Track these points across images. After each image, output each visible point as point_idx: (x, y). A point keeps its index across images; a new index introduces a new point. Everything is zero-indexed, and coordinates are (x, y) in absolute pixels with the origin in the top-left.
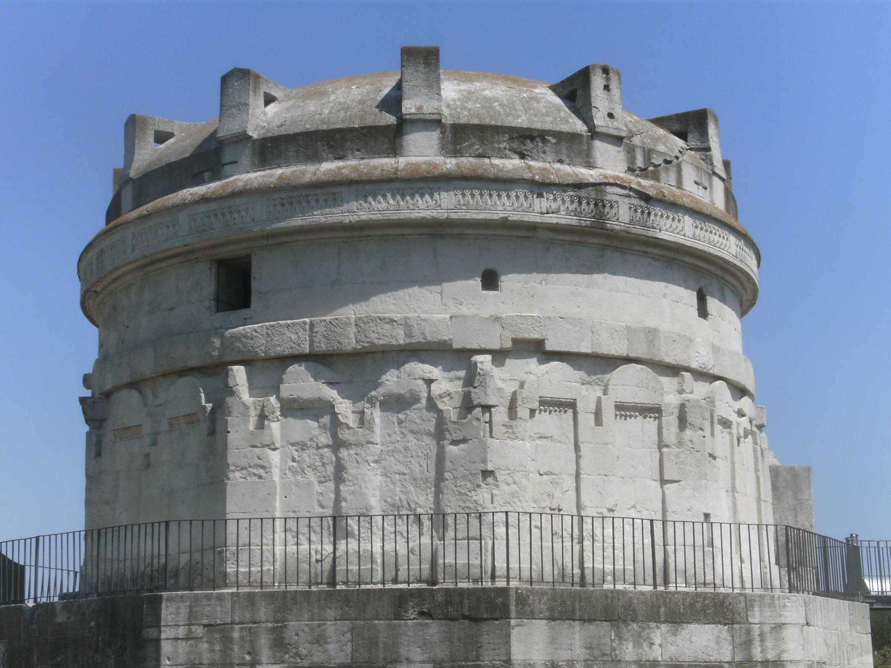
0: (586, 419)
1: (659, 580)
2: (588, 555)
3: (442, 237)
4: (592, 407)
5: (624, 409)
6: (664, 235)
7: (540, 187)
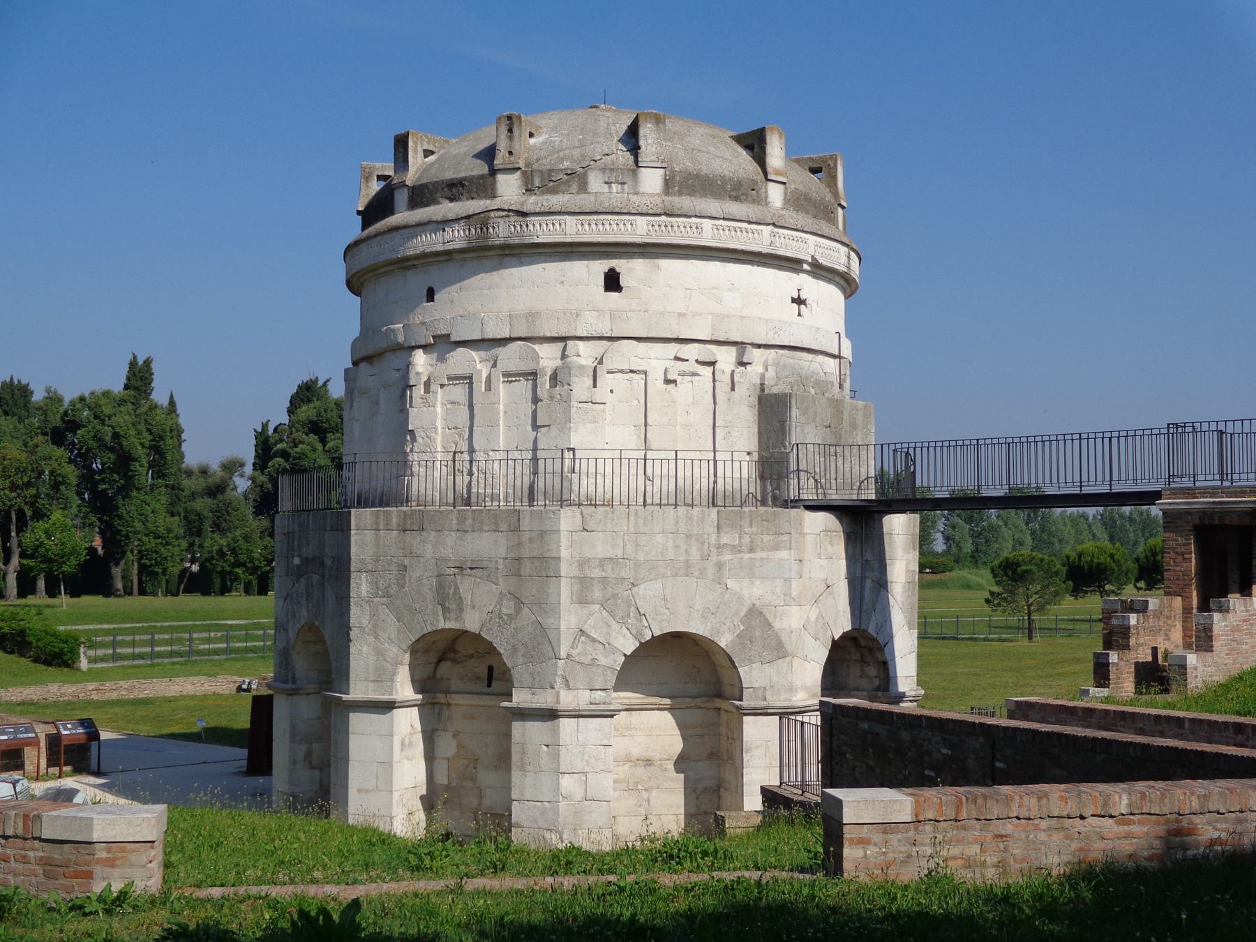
0: (480, 387)
1: (511, 499)
2: (474, 483)
3: (407, 268)
4: (484, 375)
5: (510, 376)
6: (542, 239)
7: (444, 223)
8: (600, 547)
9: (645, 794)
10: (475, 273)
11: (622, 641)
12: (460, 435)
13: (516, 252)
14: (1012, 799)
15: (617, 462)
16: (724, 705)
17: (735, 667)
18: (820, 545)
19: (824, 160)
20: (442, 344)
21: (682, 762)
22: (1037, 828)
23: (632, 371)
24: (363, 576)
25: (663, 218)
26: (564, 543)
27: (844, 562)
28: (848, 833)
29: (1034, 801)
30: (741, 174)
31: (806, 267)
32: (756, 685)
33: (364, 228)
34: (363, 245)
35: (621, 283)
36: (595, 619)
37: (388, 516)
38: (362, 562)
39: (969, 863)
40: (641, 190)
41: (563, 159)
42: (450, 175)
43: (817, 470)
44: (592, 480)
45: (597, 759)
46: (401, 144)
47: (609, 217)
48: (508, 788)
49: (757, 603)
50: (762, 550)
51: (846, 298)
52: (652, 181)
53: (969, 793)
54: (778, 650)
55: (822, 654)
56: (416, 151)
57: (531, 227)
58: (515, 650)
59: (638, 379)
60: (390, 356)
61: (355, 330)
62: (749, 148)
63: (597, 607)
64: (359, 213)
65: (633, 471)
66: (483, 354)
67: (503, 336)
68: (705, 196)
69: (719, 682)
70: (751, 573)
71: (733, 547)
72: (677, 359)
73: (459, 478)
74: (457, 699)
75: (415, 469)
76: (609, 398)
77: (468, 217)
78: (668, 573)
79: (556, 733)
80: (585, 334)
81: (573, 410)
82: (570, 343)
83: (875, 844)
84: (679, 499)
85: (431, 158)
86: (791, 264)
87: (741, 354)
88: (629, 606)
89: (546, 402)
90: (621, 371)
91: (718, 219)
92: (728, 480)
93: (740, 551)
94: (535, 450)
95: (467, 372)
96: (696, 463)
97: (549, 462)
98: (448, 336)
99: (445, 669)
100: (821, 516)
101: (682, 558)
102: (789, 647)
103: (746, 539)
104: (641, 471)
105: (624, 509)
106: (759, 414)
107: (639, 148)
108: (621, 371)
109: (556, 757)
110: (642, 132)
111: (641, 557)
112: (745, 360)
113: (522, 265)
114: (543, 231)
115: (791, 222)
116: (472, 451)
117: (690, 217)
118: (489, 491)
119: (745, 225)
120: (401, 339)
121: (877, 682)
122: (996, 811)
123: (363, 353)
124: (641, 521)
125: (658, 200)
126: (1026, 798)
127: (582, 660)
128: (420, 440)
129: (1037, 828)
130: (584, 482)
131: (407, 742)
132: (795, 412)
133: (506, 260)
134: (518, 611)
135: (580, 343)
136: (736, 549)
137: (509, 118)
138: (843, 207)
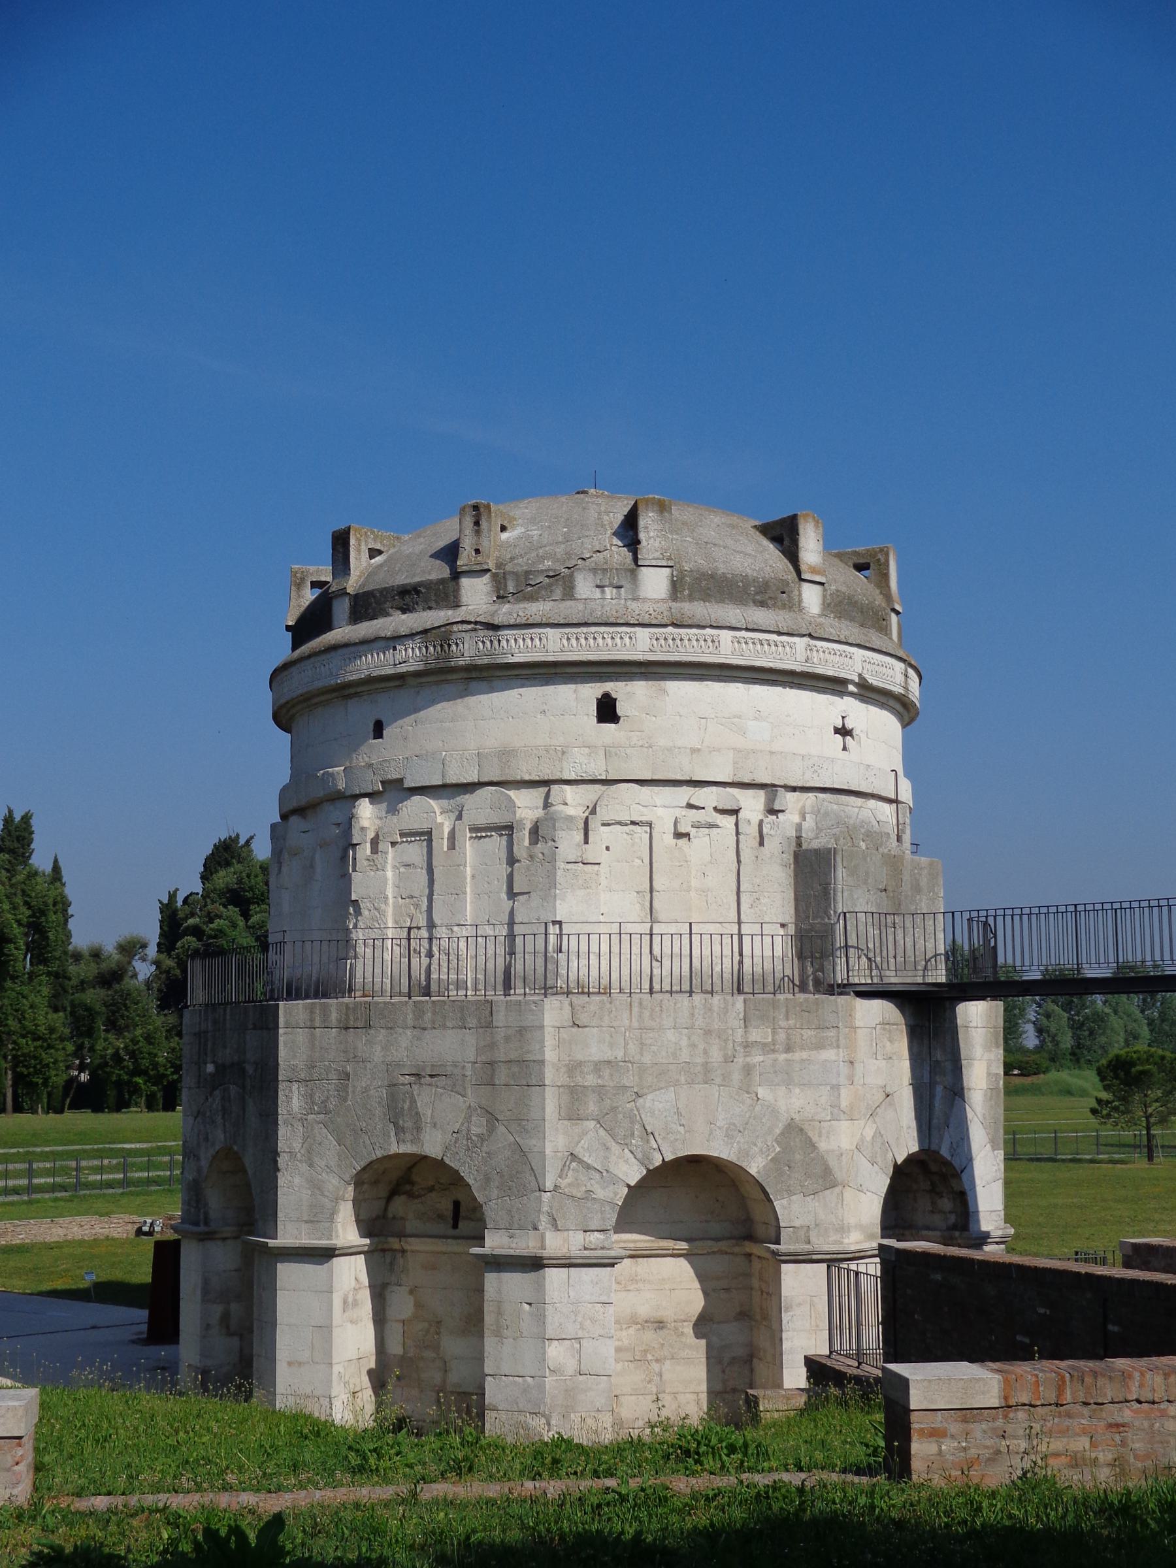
1: (481, 986)
2: (434, 967)
3: (349, 697)
4: (446, 830)
7: (394, 640)
8: (595, 1047)
9: (656, 1367)
10: (433, 702)
11: (625, 1168)
12: (417, 906)
13: (485, 674)
14: (1130, 1376)
15: (615, 938)
16: (755, 1249)
17: (770, 1201)
18: (876, 1041)
19: (873, 554)
20: (394, 791)
21: (703, 1325)
22: (1164, 1414)
23: (633, 823)
24: (295, 1086)
25: (670, 629)
26: (549, 1041)
27: (906, 1064)
28: (917, 1422)
29: (1159, 1379)
30: (768, 573)
31: (851, 688)
32: (797, 1223)
33: (294, 649)
34: (294, 670)
35: (620, 711)
36: (589, 1140)
37: (325, 1010)
38: (294, 1069)
39: (1076, 1462)
40: (642, 594)
41: (542, 559)
42: (402, 579)
43: (871, 946)
44: (583, 962)
45: (593, 1321)
46: (341, 542)
47: (602, 629)
48: (480, 1359)
49: (797, 1117)
50: (802, 1049)
51: (904, 726)
52: (655, 583)
53: (1074, 1368)
54: (825, 1178)
55: (881, 1183)
56: (359, 551)
57: (504, 643)
58: (487, 1179)
59: (641, 833)
60: (327, 807)
61: (283, 775)
62: (777, 540)
63: (591, 1124)
64: (288, 628)
65: (636, 950)
66: (445, 803)
67: (469, 780)
68: (722, 601)
69: (748, 1221)
70: (787, 1078)
71: (765, 1045)
72: (690, 806)
73: (415, 961)
74: (413, 1244)
75: (360, 949)
76: (604, 857)
77: (425, 632)
78: (683, 1079)
79: (540, 1287)
80: (573, 776)
81: (559, 873)
82: (555, 788)
83: (952, 1436)
84: (695, 985)
85: (378, 559)
86: (833, 685)
87: (771, 800)
88: (632, 1122)
89: (525, 862)
90: (620, 823)
91: (739, 629)
92: (757, 960)
93: (774, 1051)
94: (511, 923)
95: (425, 826)
96: (716, 938)
97: (529, 938)
98: (401, 781)
99: (399, 1205)
100: (877, 1004)
101: (699, 1060)
102: (839, 1175)
103: (782, 1036)
104: (646, 950)
105: (625, 997)
106: (796, 875)
107: (639, 542)
108: (620, 823)
109: (541, 1318)
110: (642, 523)
111: (647, 1059)
112: (777, 807)
113: (492, 690)
114: (519, 648)
115: (832, 632)
116: (431, 925)
117: (704, 627)
118: (453, 976)
119: (774, 637)
120: (341, 785)
121: (952, 1219)
122: (1110, 1392)
123: (294, 804)
124: (647, 1013)
125: (663, 607)
126: (1149, 1375)
127: (575, 1192)
128: (365, 913)
129: (1164, 1414)
130: (574, 964)
131: (350, 1300)
132: (841, 873)
133: (474, 685)
134: (491, 1130)
135: (567, 788)
136: (768, 1048)
137: (476, 508)
138: (898, 613)
